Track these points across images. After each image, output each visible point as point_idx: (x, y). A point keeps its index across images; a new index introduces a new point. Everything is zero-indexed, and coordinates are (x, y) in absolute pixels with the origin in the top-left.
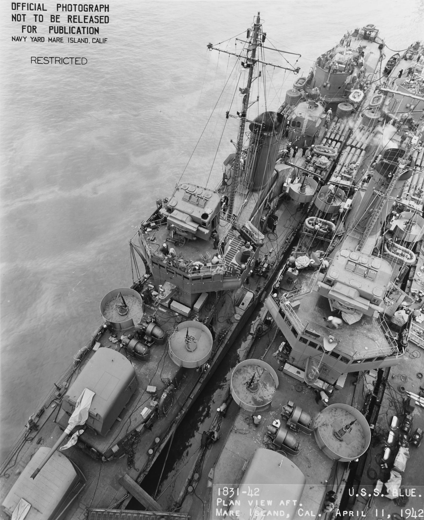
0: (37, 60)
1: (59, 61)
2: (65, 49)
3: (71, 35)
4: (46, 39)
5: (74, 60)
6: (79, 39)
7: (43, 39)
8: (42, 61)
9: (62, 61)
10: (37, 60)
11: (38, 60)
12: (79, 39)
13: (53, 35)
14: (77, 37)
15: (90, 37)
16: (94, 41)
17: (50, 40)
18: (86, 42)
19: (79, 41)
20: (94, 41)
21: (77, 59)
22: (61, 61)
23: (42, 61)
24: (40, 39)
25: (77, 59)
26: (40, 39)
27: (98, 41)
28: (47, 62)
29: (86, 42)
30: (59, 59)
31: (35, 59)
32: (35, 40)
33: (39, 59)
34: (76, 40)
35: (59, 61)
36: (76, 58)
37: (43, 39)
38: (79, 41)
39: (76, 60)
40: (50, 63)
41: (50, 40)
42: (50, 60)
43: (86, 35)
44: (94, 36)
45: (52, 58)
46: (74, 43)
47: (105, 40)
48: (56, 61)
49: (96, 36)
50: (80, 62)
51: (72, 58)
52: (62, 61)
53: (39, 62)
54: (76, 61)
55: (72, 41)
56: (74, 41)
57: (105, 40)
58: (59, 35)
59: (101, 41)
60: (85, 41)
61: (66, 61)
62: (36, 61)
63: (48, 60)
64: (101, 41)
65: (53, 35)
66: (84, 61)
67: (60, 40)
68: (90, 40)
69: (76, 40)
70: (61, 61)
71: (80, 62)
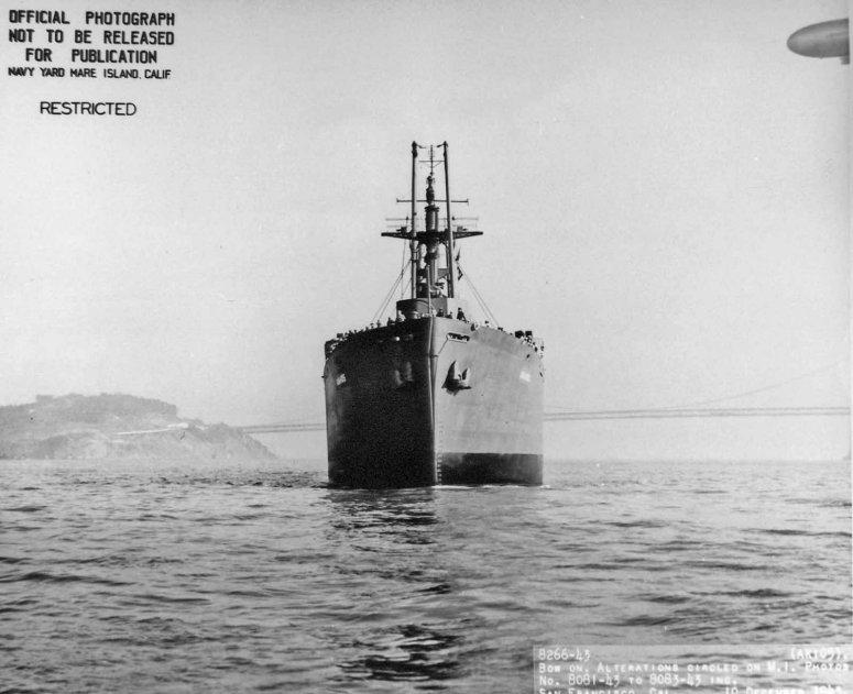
1: (88, 109)
2: (97, 88)
3: (109, 65)
4: (68, 73)
5: (113, 107)
8: (60, 108)
9: (93, 109)
13: (79, 65)
14: (119, 67)
15: (141, 68)
16: (149, 74)
17: (73, 72)
19: (124, 74)
21: (119, 106)
23: (60, 108)
24: (58, 72)
25: (119, 106)
26: (58, 72)
27: (155, 75)
28: (68, 111)
30: (86, 106)
34: (118, 75)
35: (88, 109)
38: (124, 74)
39: (116, 108)
40: (73, 109)
41: (73, 72)
42: (72, 107)
44: (148, 66)
45: (76, 104)
46: (114, 78)
47: (166, 73)
48: (83, 109)
49: (152, 66)
50: (123, 110)
51: (110, 104)
52: (93, 109)
54: (117, 109)
55: (111, 74)
56: (114, 76)
57: (166, 73)
58: (89, 65)
59: (161, 75)
60: (133, 74)
61: (100, 109)
63: (69, 108)
64: (161, 75)
65: (79, 65)
67: (91, 73)
68: (141, 74)
69: (118, 75)
71: (123, 110)
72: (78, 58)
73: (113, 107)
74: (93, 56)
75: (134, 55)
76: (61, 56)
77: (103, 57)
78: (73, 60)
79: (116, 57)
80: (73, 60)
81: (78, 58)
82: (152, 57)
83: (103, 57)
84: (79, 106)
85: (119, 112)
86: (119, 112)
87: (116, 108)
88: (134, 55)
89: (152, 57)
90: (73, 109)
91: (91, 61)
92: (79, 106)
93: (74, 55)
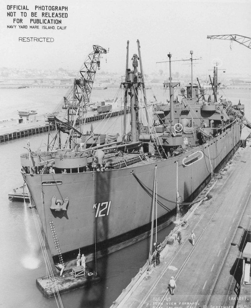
0: (22, 39)
2: (40, 32)
3: (44, 25)
4: (28, 27)
5: (46, 39)
6: (49, 27)
7: (26, 27)
8: (26, 40)
9: (38, 40)
10: (22, 39)
11: (23, 39)
12: (49, 27)
14: (48, 25)
15: (56, 25)
16: (59, 28)
18: (54, 28)
19: (49, 28)
20: (59, 28)
21: (47, 39)
22: (37, 40)
23: (26, 40)
24: (25, 27)
26: (25, 27)
28: (29, 40)
29: (54, 28)
30: (35, 39)
31: (21, 39)
32: (22, 27)
33: (24, 39)
34: (47, 28)
36: (47, 38)
37: (26, 27)
39: (47, 39)
40: (31, 40)
43: (53, 25)
45: (32, 38)
47: (65, 28)
49: (60, 25)
51: (44, 38)
52: (38, 40)
53: (24, 40)
54: (47, 40)
55: (45, 28)
57: (65, 28)
58: (36, 24)
60: (53, 28)
62: (22, 40)
64: (63, 28)
65: (33, 24)
66: (52, 40)
67: (37, 27)
68: (56, 28)
69: (47, 28)
70: (37, 40)
71: (49, 40)
72: (32, 22)
73: (46, 39)
74: (38, 21)
75: (53, 21)
76: (26, 21)
77: (42, 22)
78: (31, 23)
79: (46, 22)
80: (31, 23)
81: (32, 22)
82: (60, 22)
83: (42, 22)
84: (33, 39)
85: (47, 41)
86: (47, 41)
87: (47, 39)
88: (53, 21)
89: (60, 22)
90: (31, 40)
91: (37, 23)
92: (33, 39)
93: (31, 21)
